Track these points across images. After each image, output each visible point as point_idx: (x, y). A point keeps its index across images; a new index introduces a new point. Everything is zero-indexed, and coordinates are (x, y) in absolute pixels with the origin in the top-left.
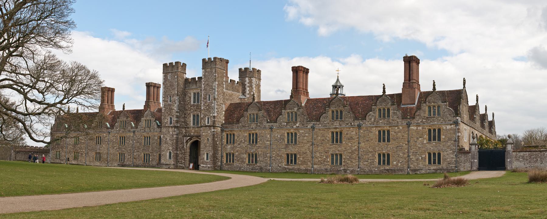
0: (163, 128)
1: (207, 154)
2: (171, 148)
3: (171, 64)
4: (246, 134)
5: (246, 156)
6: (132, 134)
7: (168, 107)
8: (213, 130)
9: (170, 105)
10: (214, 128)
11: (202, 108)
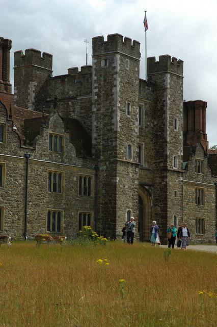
0: (119, 163)
1: (175, 217)
2: (130, 204)
3: (128, 40)
4: (194, 190)
5: (194, 222)
6: (21, 165)
7: (127, 123)
8: (181, 179)
9: (128, 120)
10: (182, 176)
11: (168, 140)
